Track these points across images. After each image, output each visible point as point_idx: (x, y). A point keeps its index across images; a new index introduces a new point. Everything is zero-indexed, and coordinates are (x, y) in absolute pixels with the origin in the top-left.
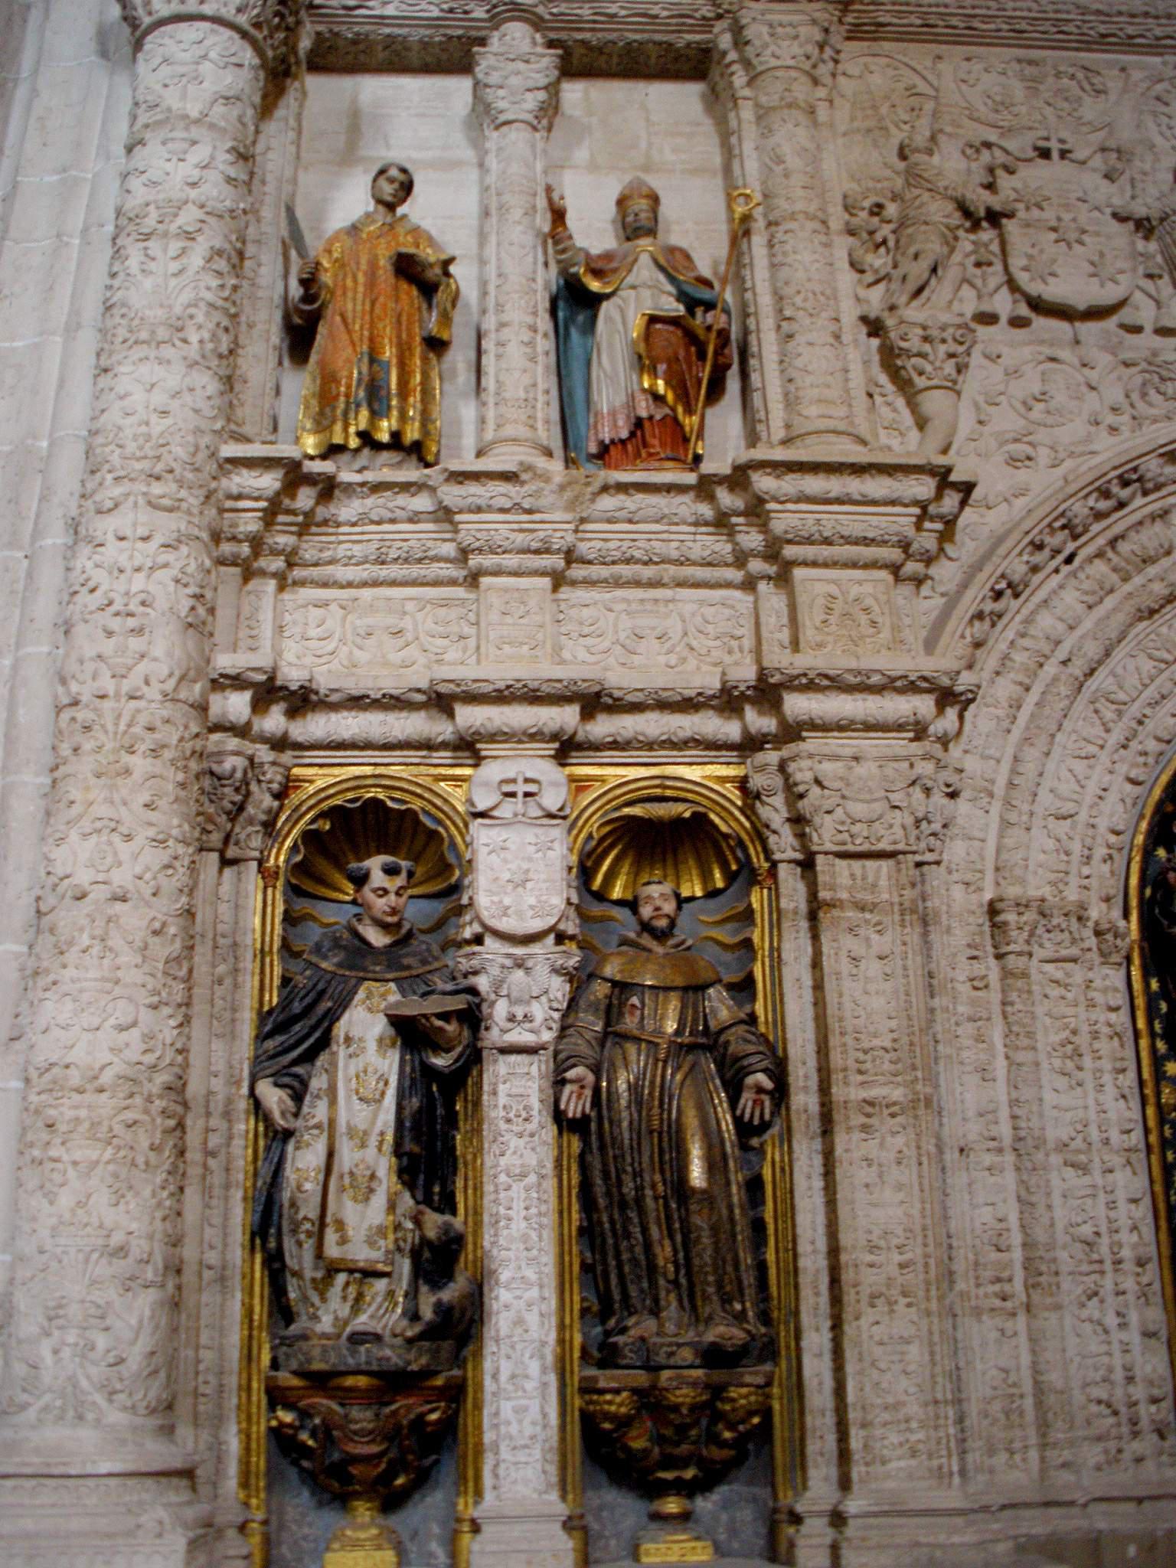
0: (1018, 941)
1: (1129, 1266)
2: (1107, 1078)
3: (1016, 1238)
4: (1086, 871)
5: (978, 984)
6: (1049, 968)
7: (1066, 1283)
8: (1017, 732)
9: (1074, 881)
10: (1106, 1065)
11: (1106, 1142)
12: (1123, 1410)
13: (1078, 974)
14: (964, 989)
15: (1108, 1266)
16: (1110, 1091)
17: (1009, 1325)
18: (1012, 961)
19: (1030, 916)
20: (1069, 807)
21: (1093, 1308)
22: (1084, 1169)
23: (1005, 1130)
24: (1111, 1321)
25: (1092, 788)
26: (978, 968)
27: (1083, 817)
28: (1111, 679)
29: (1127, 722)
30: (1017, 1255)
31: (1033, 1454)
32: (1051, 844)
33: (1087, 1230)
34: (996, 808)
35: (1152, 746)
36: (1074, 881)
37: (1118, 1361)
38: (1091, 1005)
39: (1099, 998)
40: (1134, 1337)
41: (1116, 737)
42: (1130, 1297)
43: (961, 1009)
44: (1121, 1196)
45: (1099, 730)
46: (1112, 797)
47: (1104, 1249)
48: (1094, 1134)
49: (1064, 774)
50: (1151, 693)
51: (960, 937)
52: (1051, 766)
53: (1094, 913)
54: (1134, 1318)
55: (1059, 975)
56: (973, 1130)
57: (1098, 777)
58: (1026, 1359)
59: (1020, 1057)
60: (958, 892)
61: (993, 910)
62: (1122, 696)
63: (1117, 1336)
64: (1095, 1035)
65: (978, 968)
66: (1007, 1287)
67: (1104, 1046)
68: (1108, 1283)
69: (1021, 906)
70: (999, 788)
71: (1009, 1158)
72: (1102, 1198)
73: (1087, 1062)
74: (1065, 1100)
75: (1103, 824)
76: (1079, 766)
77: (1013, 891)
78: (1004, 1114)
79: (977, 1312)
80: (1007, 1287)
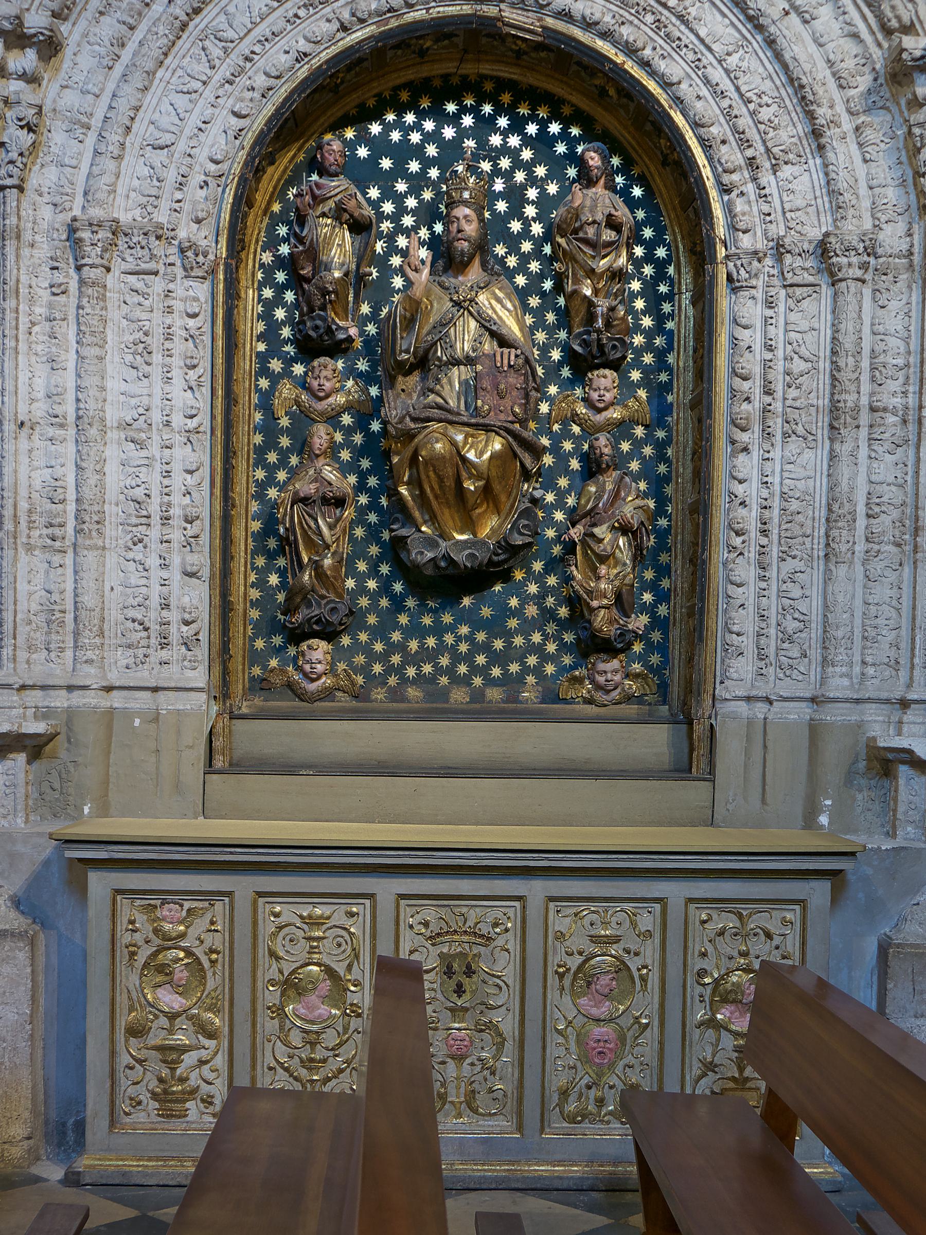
0: (92, 255)
1: (177, 523)
2: (176, 373)
3: (71, 495)
4: (178, 195)
5: (58, 290)
6: (132, 279)
7: (110, 530)
8: (119, 69)
9: (165, 204)
10: (177, 362)
11: (168, 424)
12: (154, 628)
13: (158, 285)
14: (45, 295)
15: (156, 520)
16: (178, 383)
17: (57, 559)
18: (90, 274)
19: (103, 234)
20: (167, 139)
21: (137, 553)
22: (140, 444)
23: (70, 409)
24: (153, 561)
25: (194, 121)
26: (59, 277)
27: (182, 146)
28: (222, 18)
29: (235, 58)
30: (71, 507)
31: (69, 654)
32: (146, 171)
33: (139, 493)
34: (91, 139)
35: (261, 81)
36: (165, 204)
37: (155, 591)
38: (169, 310)
39: (178, 305)
40: (176, 576)
41: (224, 71)
42: (175, 545)
43: (38, 310)
44: (177, 468)
45: (204, 67)
46: (215, 130)
47: (154, 507)
48: (156, 417)
49: (165, 107)
50: (263, 29)
51: (43, 251)
52: (150, 99)
53: (182, 234)
54: (176, 561)
55: (139, 285)
56: (40, 409)
57: (202, 110)
58: (69, 586)
59: (85, 352)
60: (47, 213)
61: (72, 230)
62: (230, 34)
63: (157, 574)
64: (169, 337)
65: (59, 277)
66: (57, 531)
67: (179, 346)
68: (155, 533)
69: (95, 225)
70: (96, 122)
71: (72, 431)
72: (158, 467)
73: (157, 358)
74: (134, 388)
75: (202, 155)
76: (182, 102)
77: (96, 213)
78: (71, 396)
79: (29, 548)
80: (57, 531)
